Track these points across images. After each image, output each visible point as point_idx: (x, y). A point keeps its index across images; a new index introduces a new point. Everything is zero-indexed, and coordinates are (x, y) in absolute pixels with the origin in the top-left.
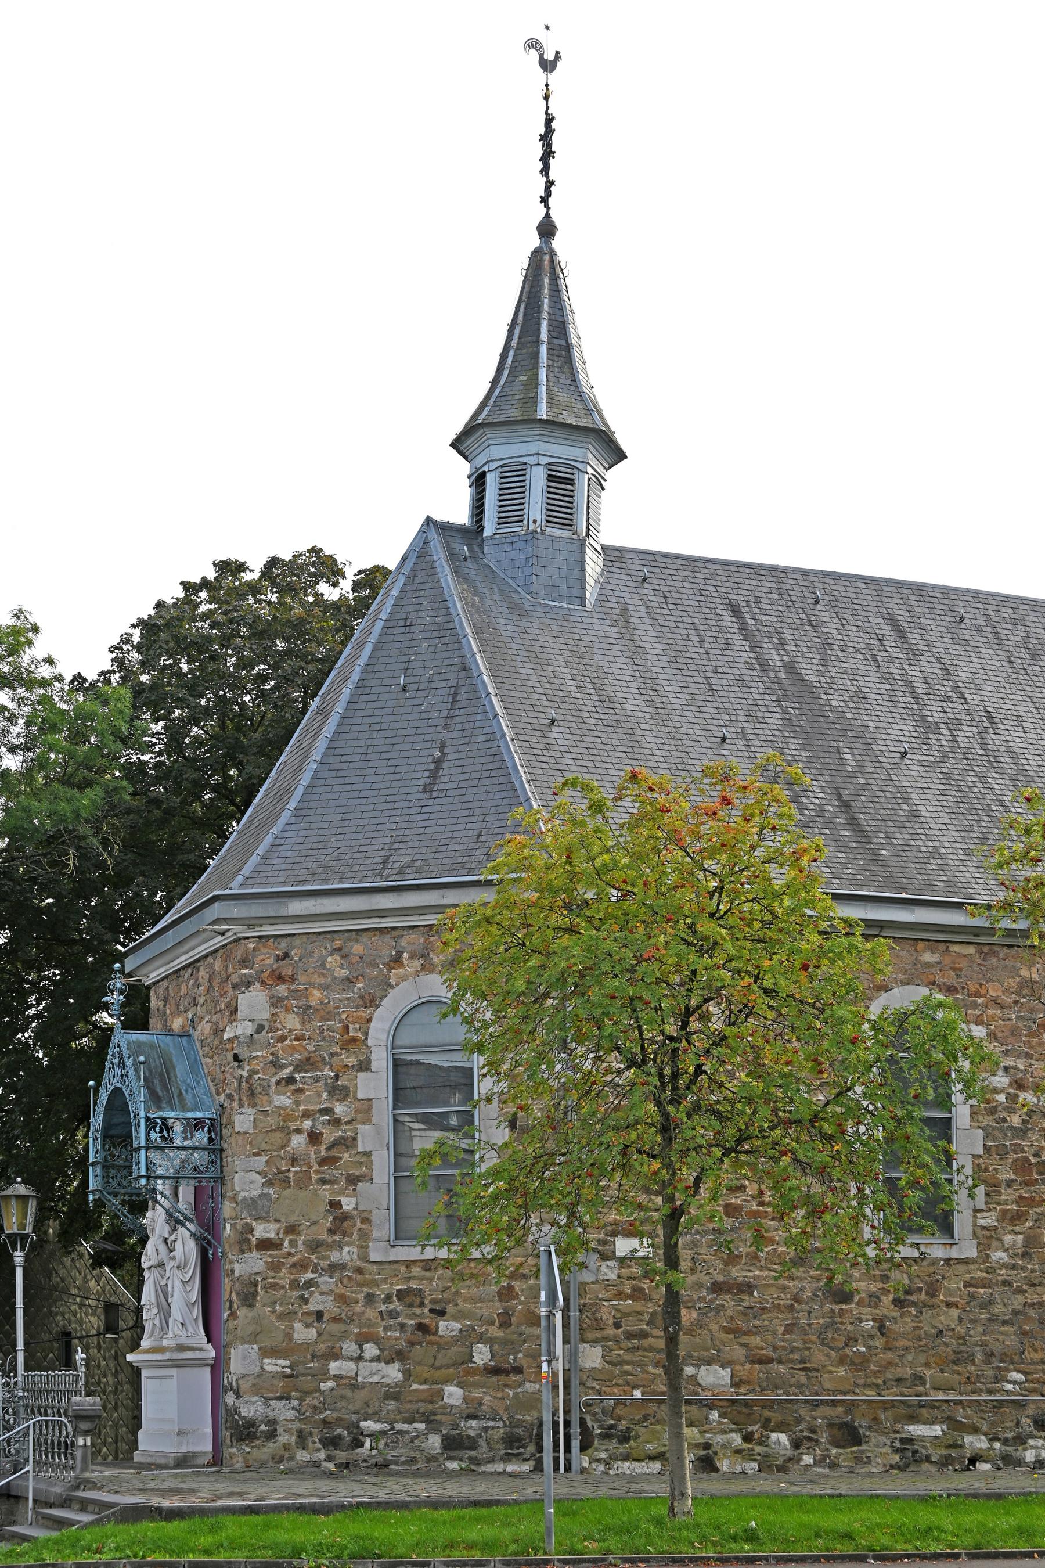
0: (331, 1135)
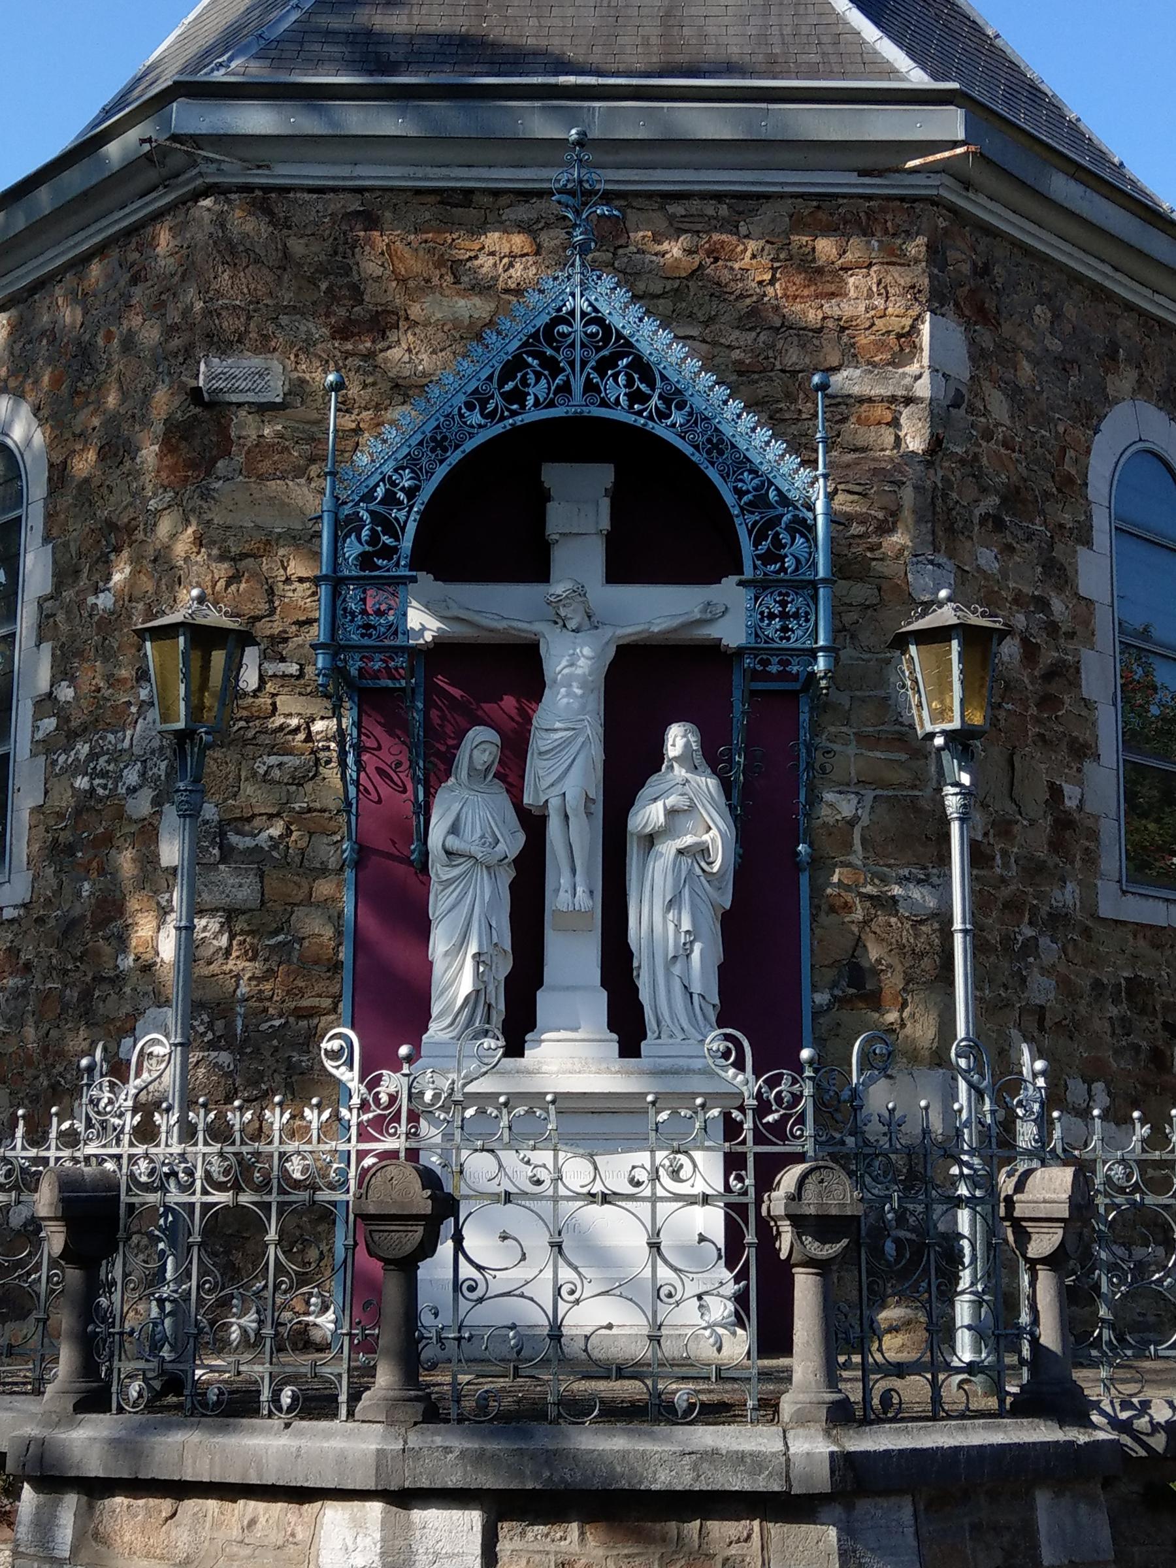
0: (1049, 656)
